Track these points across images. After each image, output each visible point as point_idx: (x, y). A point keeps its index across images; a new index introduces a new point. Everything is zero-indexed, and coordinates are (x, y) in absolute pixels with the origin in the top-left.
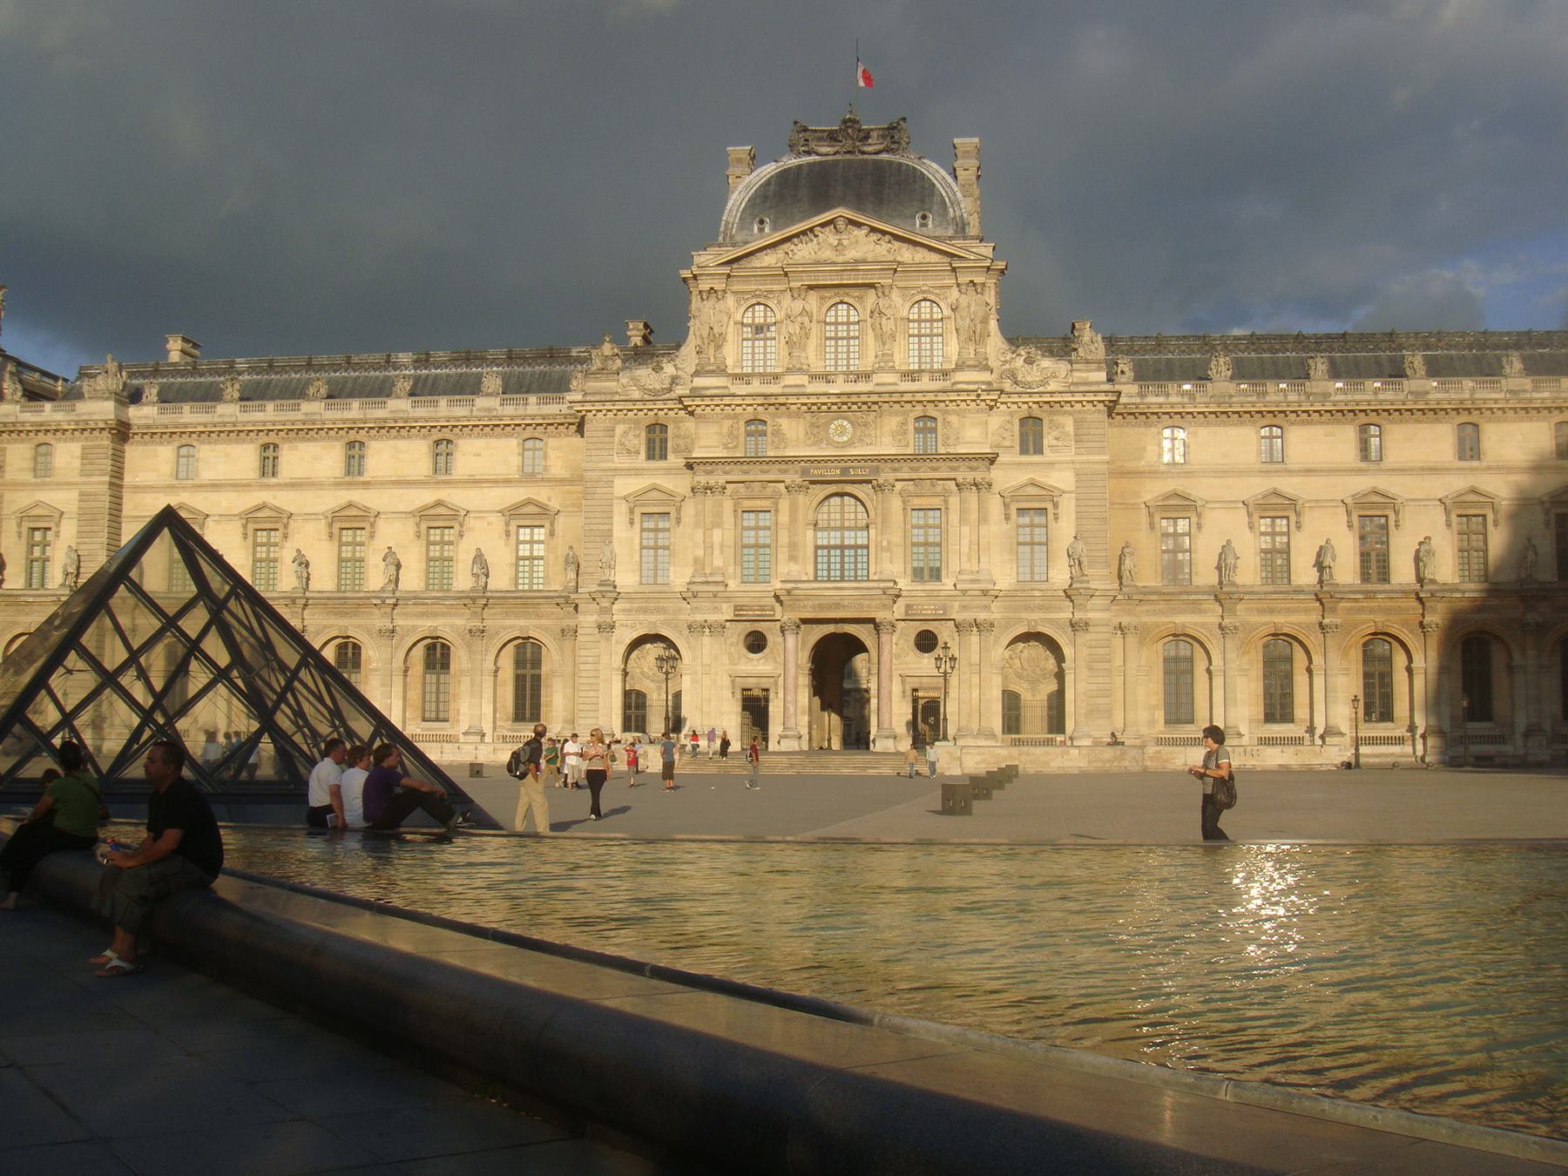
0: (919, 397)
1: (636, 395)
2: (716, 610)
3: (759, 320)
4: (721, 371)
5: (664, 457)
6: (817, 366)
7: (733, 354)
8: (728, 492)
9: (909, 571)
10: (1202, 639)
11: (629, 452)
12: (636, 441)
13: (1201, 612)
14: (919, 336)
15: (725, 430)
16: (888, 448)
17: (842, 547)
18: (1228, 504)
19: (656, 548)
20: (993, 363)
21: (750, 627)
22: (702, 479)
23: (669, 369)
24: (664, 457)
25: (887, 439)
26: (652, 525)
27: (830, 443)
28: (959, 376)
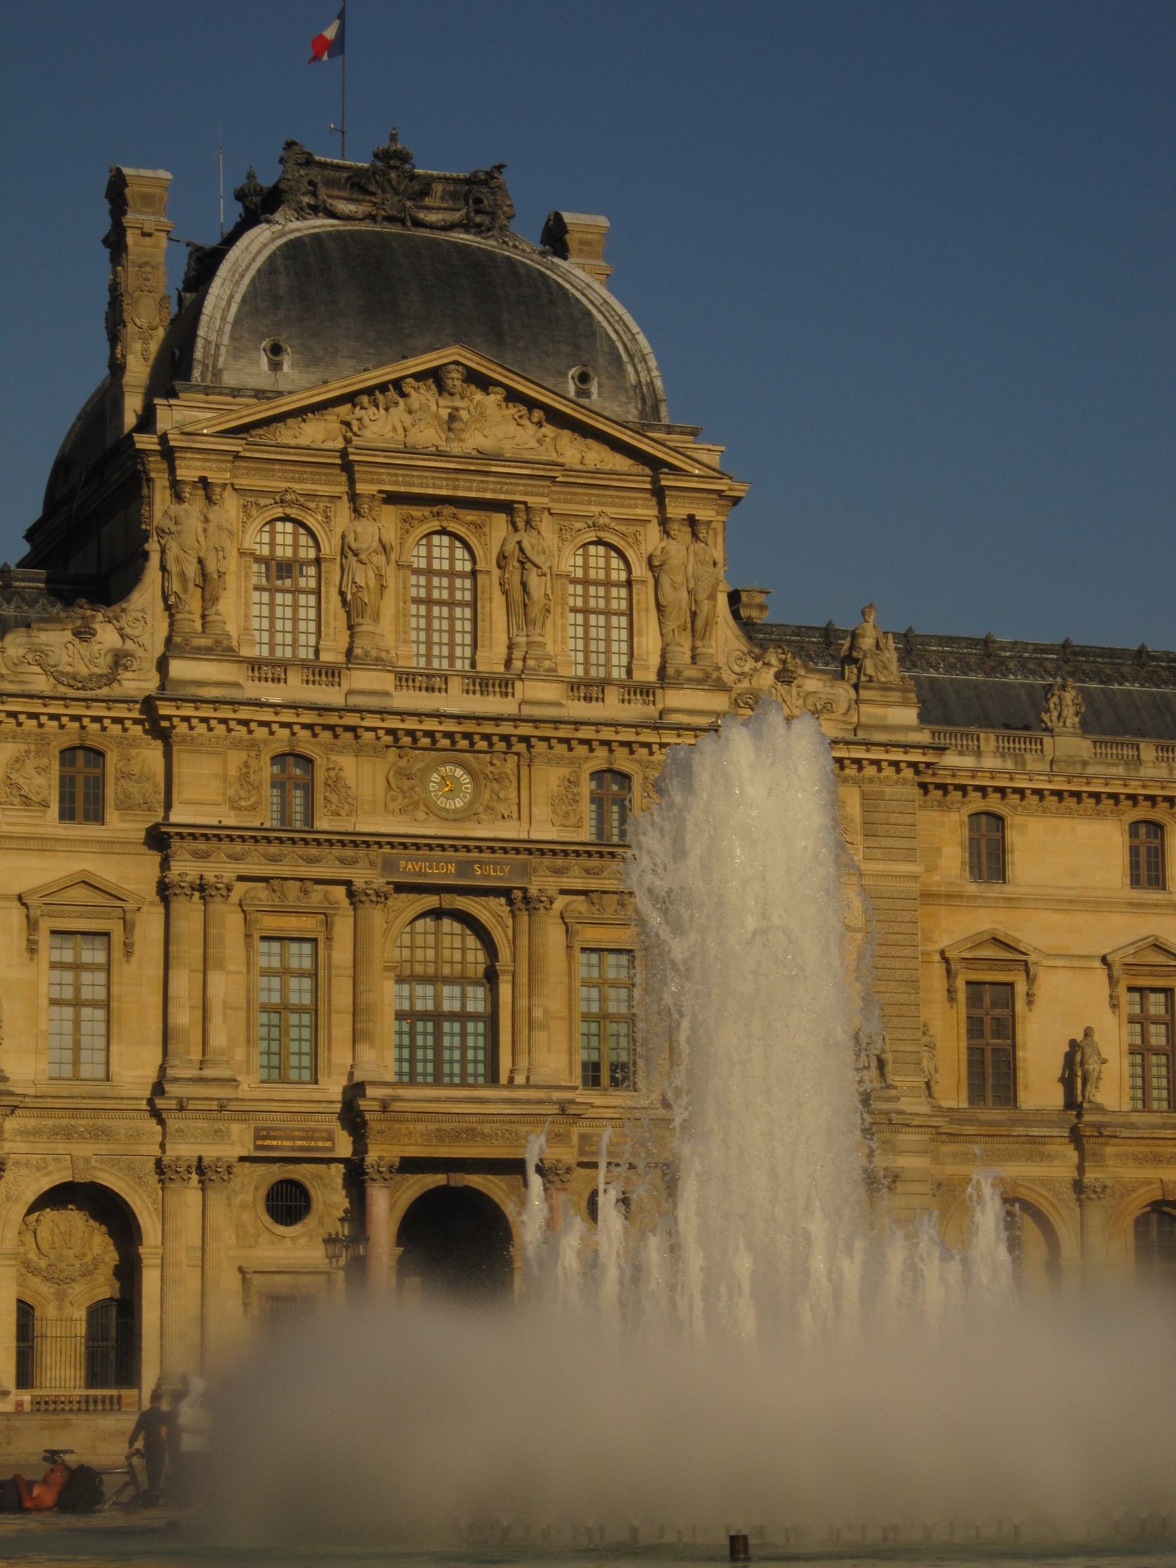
0: (607, 734)
1: (41, 684)
2: (219, 1135)
3: (284, 552)
4: (223, 651)
5: (96, 815)
6: (411, 657)
7: (244, 611)
8: (235, 897)
9: (578, 1070)
10: (1045, 1207)
11: (26, 801)
12: (40, 780)
13: (1045, 1158)
14: (586, 611)
15: (233, 772)
16: (545, 831)
17: (437, 1017)
18: (1076, 961)
19: (77, 1003)
20: (728, 677)
21: (277, 1172)
22: (185, 868)
23: (107, 636)
24: (96, 815)
25: (541, 811)
26: (68, 956)
27: (432, 811)
28: (674, 699)
